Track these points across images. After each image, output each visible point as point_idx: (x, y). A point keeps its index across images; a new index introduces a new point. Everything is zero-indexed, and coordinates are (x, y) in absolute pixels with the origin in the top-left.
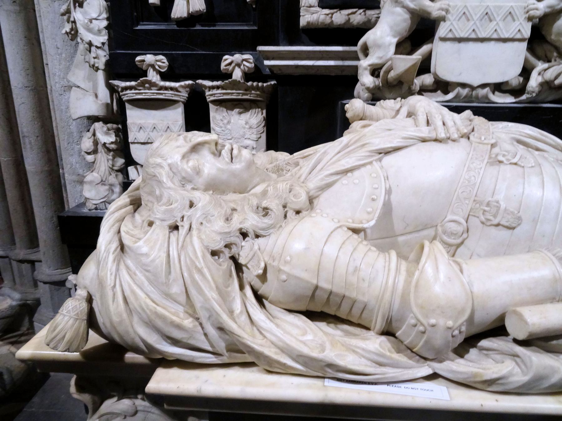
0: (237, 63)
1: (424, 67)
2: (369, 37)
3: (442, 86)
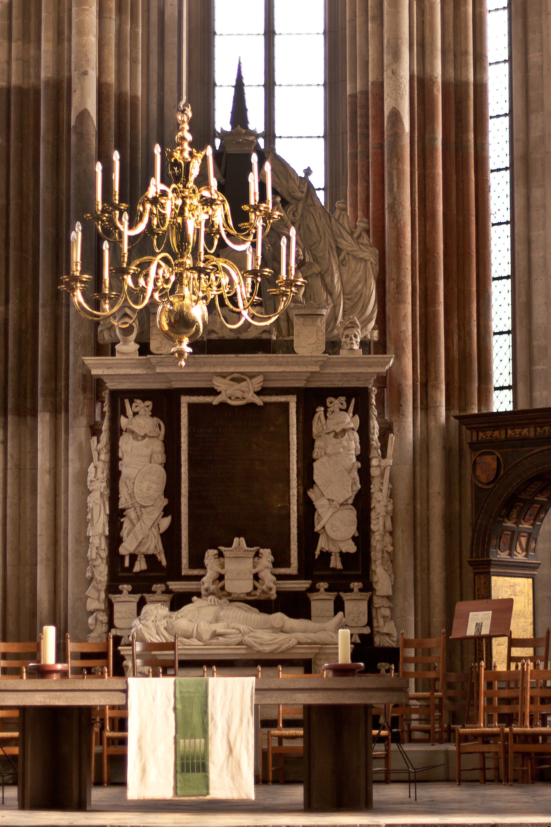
0: (158, 587)
1: (223, 588)
2: (204, 579)
3: (229, 594)
